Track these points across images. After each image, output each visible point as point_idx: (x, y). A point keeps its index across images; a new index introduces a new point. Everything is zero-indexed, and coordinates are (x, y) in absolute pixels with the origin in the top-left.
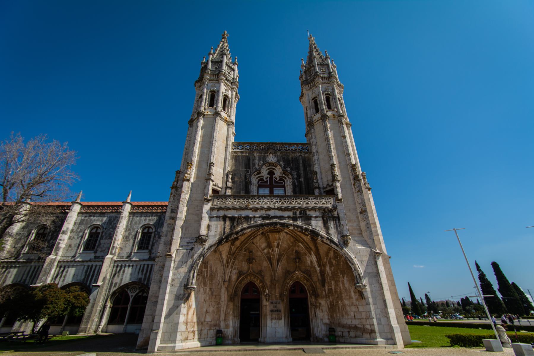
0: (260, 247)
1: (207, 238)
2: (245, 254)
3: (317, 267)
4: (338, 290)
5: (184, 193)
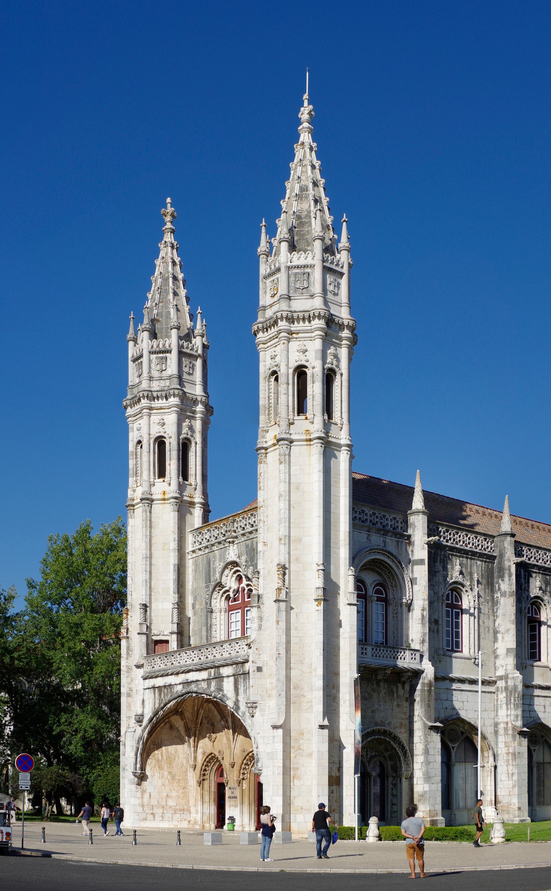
1: (141, 717)
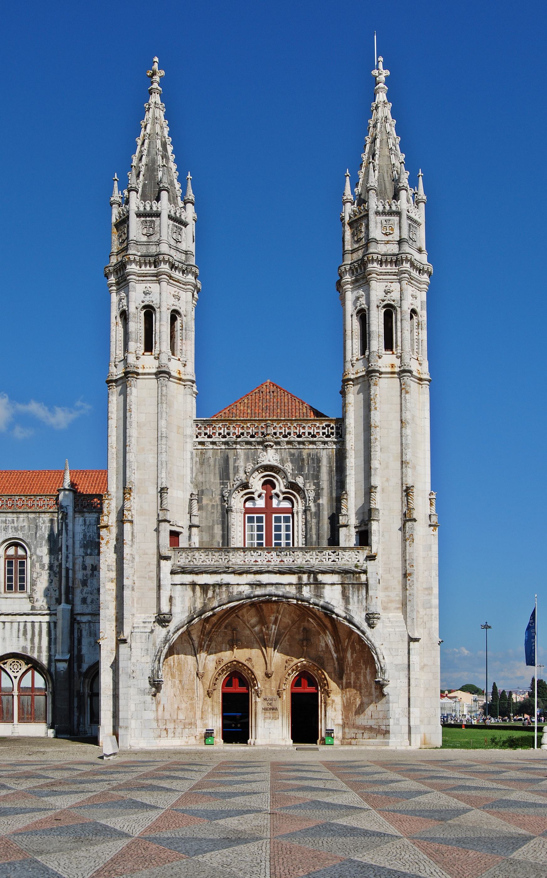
0: (248, 623)
2: (225, 633)
3: (333, 653)
4: (358, 685)
5: (128, 546)
